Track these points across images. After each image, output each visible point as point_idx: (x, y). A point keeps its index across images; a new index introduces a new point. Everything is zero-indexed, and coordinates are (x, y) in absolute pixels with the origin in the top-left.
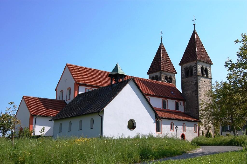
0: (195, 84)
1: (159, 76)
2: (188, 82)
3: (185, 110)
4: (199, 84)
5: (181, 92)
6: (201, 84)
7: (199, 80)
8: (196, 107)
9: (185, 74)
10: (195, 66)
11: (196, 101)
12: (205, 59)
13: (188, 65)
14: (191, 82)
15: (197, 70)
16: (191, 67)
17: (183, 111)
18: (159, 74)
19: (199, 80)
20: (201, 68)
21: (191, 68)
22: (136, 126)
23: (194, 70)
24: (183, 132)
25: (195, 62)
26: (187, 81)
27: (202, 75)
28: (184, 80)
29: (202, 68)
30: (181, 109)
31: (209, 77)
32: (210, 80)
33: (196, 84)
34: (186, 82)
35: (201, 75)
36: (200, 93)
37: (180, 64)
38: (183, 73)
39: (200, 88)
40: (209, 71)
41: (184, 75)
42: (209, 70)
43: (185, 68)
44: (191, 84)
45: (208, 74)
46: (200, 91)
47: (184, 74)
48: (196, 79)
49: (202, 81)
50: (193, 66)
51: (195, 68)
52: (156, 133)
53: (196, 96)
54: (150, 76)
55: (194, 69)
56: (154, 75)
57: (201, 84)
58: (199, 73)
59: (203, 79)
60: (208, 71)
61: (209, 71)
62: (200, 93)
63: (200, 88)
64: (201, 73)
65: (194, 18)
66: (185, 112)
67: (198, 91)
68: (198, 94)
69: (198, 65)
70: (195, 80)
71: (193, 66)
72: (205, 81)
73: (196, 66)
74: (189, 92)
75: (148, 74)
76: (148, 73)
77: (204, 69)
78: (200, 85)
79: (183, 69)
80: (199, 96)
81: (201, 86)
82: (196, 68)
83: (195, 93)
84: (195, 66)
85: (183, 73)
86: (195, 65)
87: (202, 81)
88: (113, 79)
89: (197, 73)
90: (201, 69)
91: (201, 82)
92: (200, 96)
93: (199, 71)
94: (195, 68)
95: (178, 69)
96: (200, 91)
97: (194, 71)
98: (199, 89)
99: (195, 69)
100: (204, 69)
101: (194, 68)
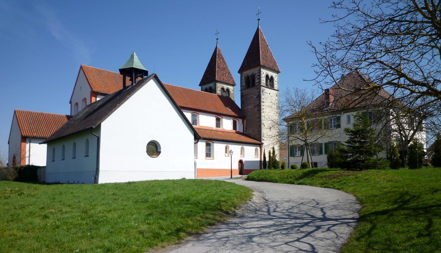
0: (257, 97)
1: (213, 88)
2: (248, 94)
3: (245, 129)
5: (240, 107)
6: (265, 97)
7: (262, 92)
8: (258, 126)
9: (246, 84)
10: (258, 73)
11: (258, 118)
12: (271, 65)
13: (249, 72)
14: (253, 94)
15: (260, 79)
16: (253, 75)
17: (242, 132)
18: (214, 86)
19: (262, 92)
20: (265, 76)
21: (253, 76)
22: (161, 151)
23: (256, 79)
24: (241, 157)
25: (258, 68)
26: (247, 93)
28: (244, 93)
29: (267, 76)
30: (240, 128)
31: (275, 89)
32: (276, 92)
33: (259, 97)
34: (247, 95)
36: (263, 109)
37: (239, 72)
38: (243, 82)
39: (263, 102)
40: (276, 81)
41: (244, 86)
43: (245, 77)
44: (253, 97)
45: (274, 84)
46: (264, 106)
47: (244, 84)
48: (258, 91)
49: (266, 93)
50: (256, 74)
51: (257, 76)
52: (206, 159)
53: (259, 112)
54: (203, 88)
55: (257, 77)
56: (207, 86)
57: (265, 97)
58: (263, 83)
59: (267, 90)
60: (274, 81)
62: (263, 109)
63: (263, 102)
64: (265, 83)
65: (258, 11)
66: (245, 132)
67: (261, 106)
68: (261, 109)
70: (258, 92)
71: (255, 73)
72: (269, 94)
73: (259, 74)
74: (249, 107)
75: (200, 85)
76: (201, 84)
77: (270, 77)
78: (264, 99)
79: (244, 78)
80: (262, 112)
82: (260, 76)
83: (258, 109)
84: (258, 73)
85: (243, 82)
86: (258, 72)
87: (266, 93)
88: (128, 79)
89: (260, 82)
90: (265, 78)
91: (264, 94)
92: (263, 112)
93: (263, 80)
94: (257, 76)
95: (237, 78)
96: (264, 106)
97: (257, 81)
98: (262, 104)
99: (258, 77)
100: (270, 77)
101: (256, 76)
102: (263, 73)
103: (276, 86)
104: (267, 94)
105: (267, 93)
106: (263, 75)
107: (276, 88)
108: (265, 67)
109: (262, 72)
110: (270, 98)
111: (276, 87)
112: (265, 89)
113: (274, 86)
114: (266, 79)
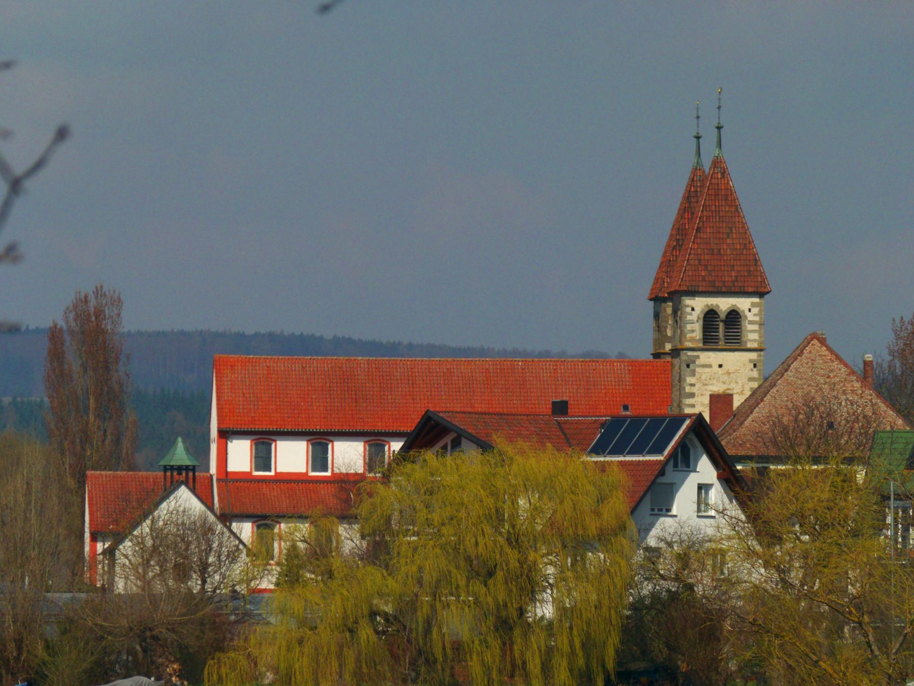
4: (690, 380)
7: (688, 366)
20: (702, 316)
27: (705, 343)
32: (753, 356)
35: (701, 345)
39: (692, 395)
40: (751, 322)
42: (750, 316)
58: (692, 340)
61: (751, 322)
63: (692, 395)
69: (689, 310)
72: (720, 366)
77: (723, 316)
78: (693, 385)
81: (698, 386)
90: (701, 322)
91: (698, 370)
93: (693, 331)
96: (693, 406)
102: (693, 309)
103: (752, 335)
104: (707, 370)
105: (710, 366)
106: (689, 317)
107: (750, 345)
108: (693, 293)
109: (688, 306)
110: (726, 378)
111: (754, 341)
112: (698, 357)
113: (744, 339)
114: (704, 325)
